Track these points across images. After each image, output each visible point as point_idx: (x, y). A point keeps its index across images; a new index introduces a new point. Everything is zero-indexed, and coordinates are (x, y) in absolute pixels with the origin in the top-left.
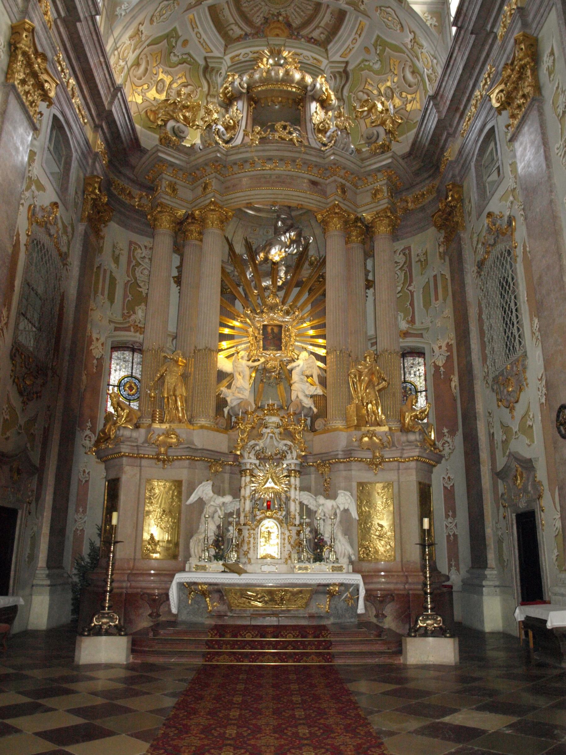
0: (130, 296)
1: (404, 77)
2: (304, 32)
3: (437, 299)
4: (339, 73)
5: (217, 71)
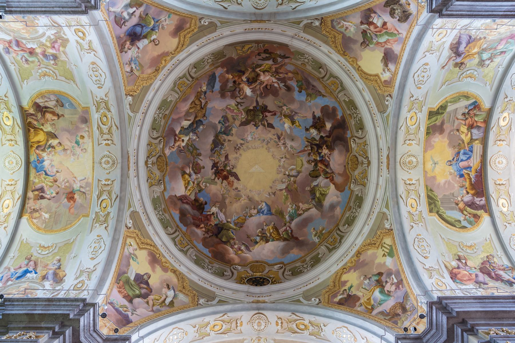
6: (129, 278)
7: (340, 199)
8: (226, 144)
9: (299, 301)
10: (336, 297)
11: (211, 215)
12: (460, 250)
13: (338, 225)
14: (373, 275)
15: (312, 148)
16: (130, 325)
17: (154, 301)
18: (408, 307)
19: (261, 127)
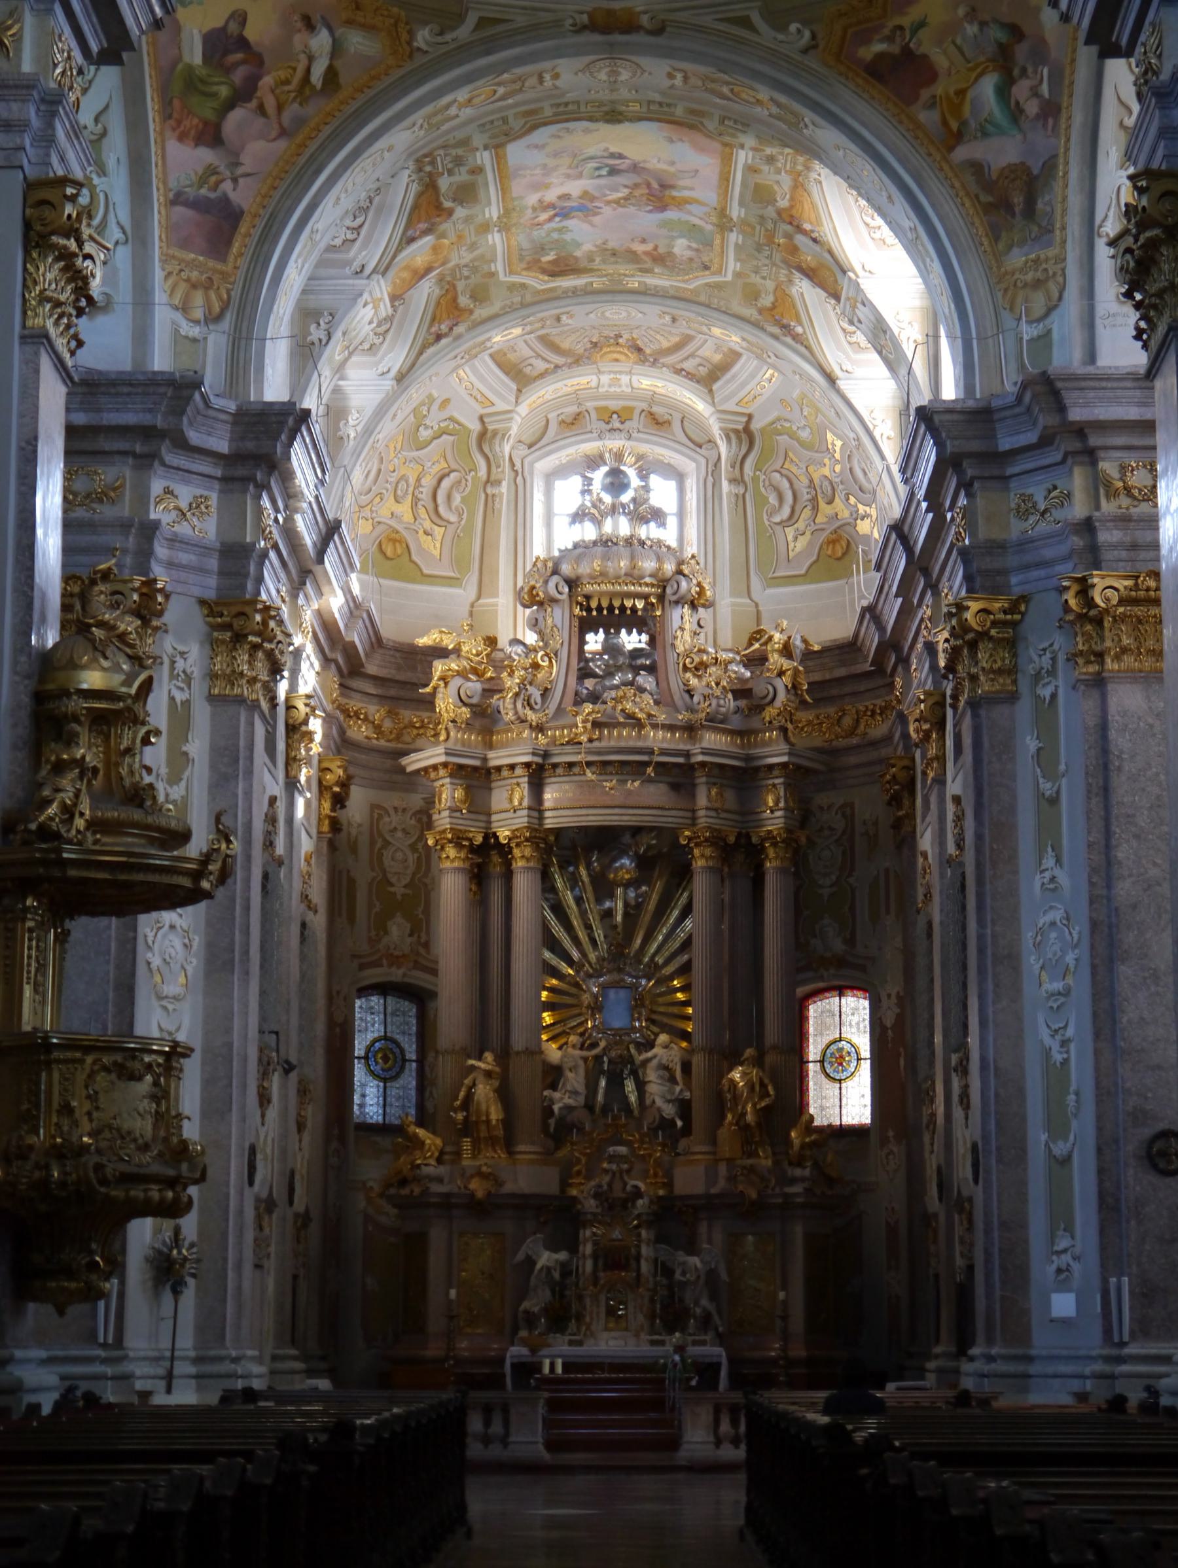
0: (378, 904)
1: (851, 469)
2: (670, 360)
3: (888, 912)
4: (736, 432)
5: (504, 436)
6: (190, 68)
9: (745, 22)
10: (867, 41)
14: (995, 21)
16: (243, 229)
17: (278, 91)
18: (1040, 205)
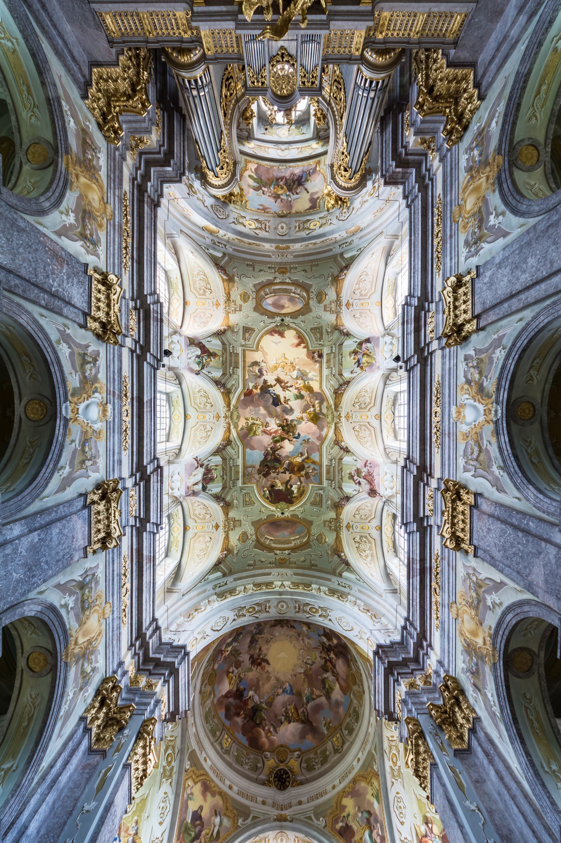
6: (187, 823)
7: (343, 700)
8: (260, 640)
11: (248, 699)
12: (428, 810)
13: (341, 725)
15: (323, 649)
19: (285, 628)
